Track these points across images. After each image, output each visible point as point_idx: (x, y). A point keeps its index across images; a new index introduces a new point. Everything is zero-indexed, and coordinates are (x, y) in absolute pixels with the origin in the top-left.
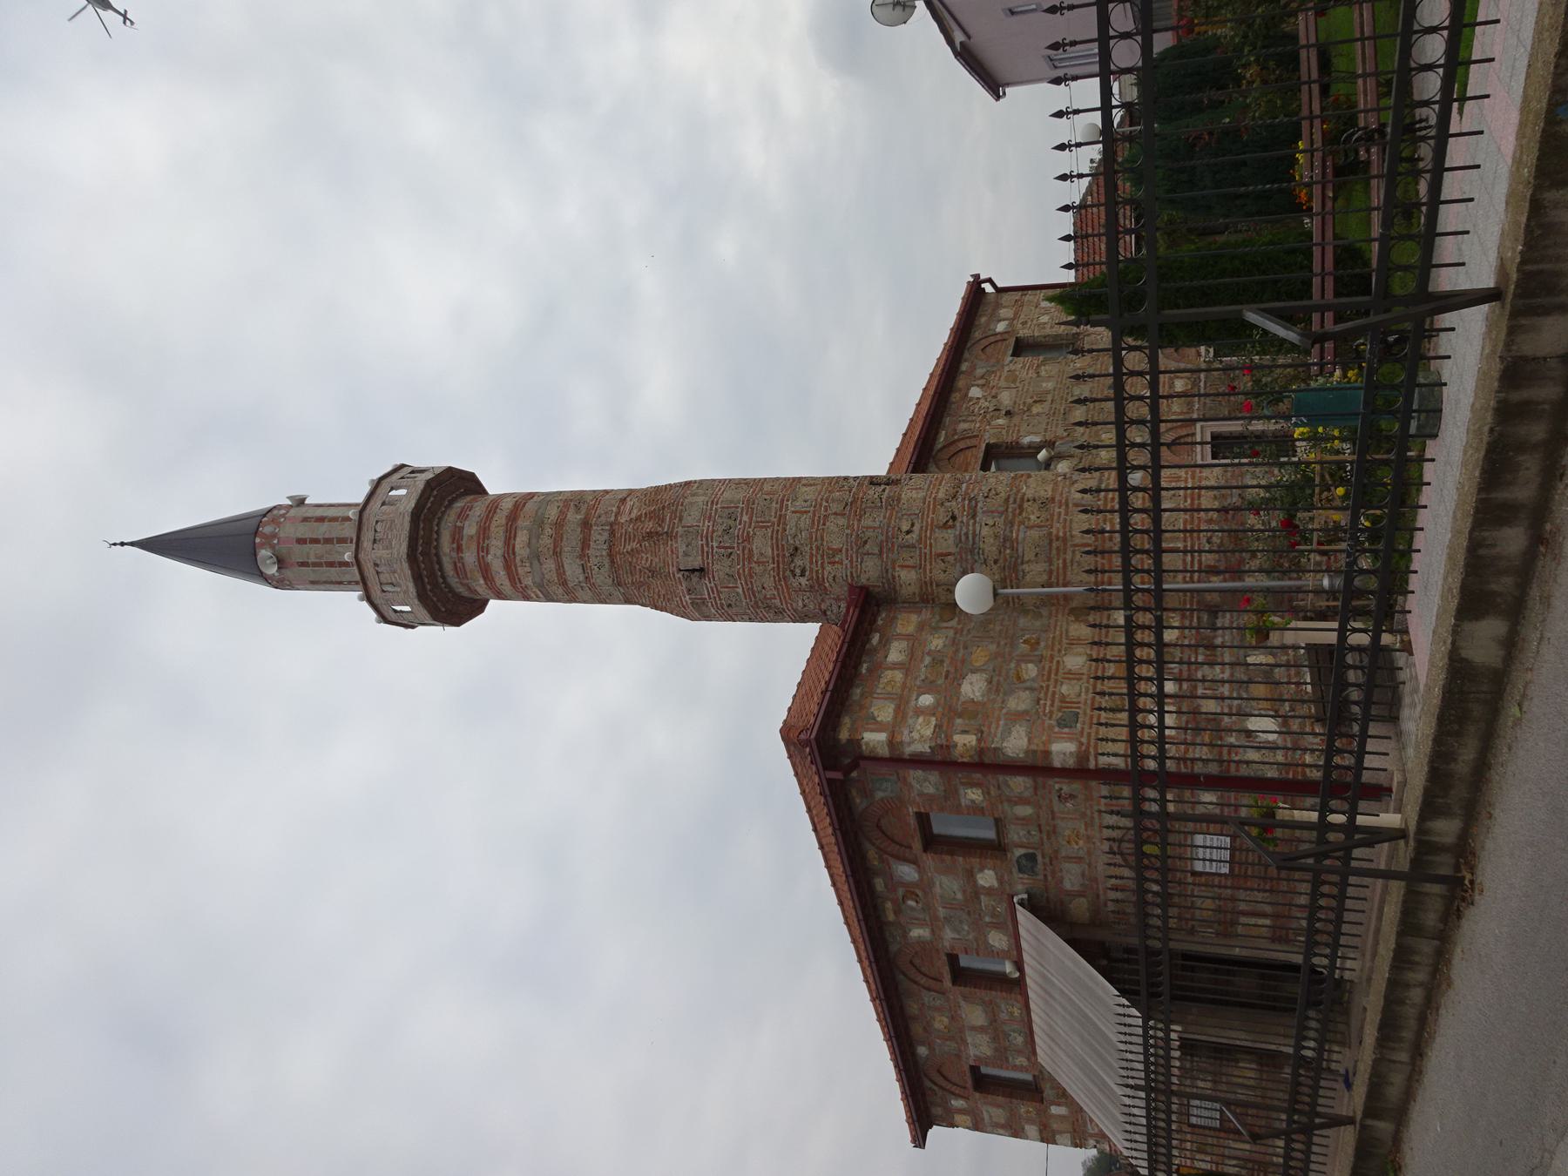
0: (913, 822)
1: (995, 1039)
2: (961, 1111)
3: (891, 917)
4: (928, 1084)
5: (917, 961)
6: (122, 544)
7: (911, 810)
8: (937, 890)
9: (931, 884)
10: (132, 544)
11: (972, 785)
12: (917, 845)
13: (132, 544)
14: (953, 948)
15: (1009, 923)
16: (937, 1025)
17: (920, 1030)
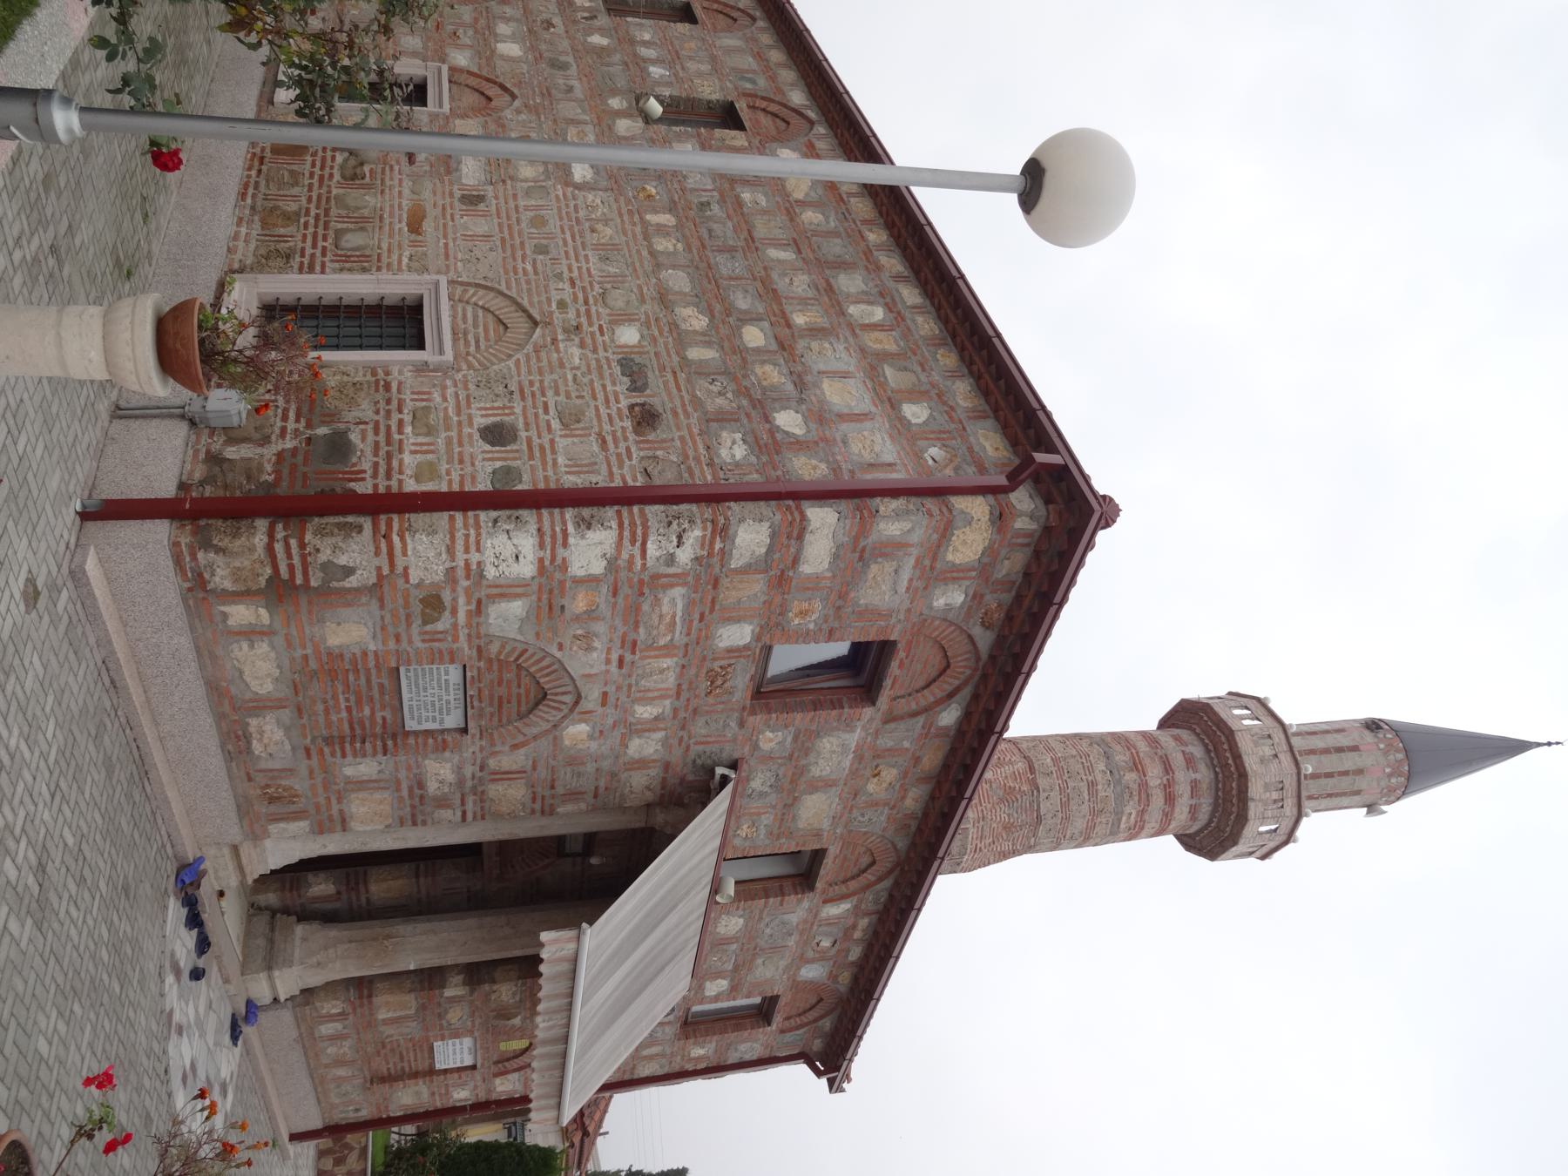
0: (778, 1019)
1: (803, 771)
2: (953, 574)
3: (864, 922)
4: (984, 639)
5: (865, 860)
6: (1549, 744)
7: (774, 1027)
8: (783, 963)
9: (787, 968)
10: (1539, 745)
11: (699, 1059)
12: (782, 1003)
13: (1539, 745)
14: (800, 901)
15: (707, 945)
16: (889, 774)
17: (925, 760)
